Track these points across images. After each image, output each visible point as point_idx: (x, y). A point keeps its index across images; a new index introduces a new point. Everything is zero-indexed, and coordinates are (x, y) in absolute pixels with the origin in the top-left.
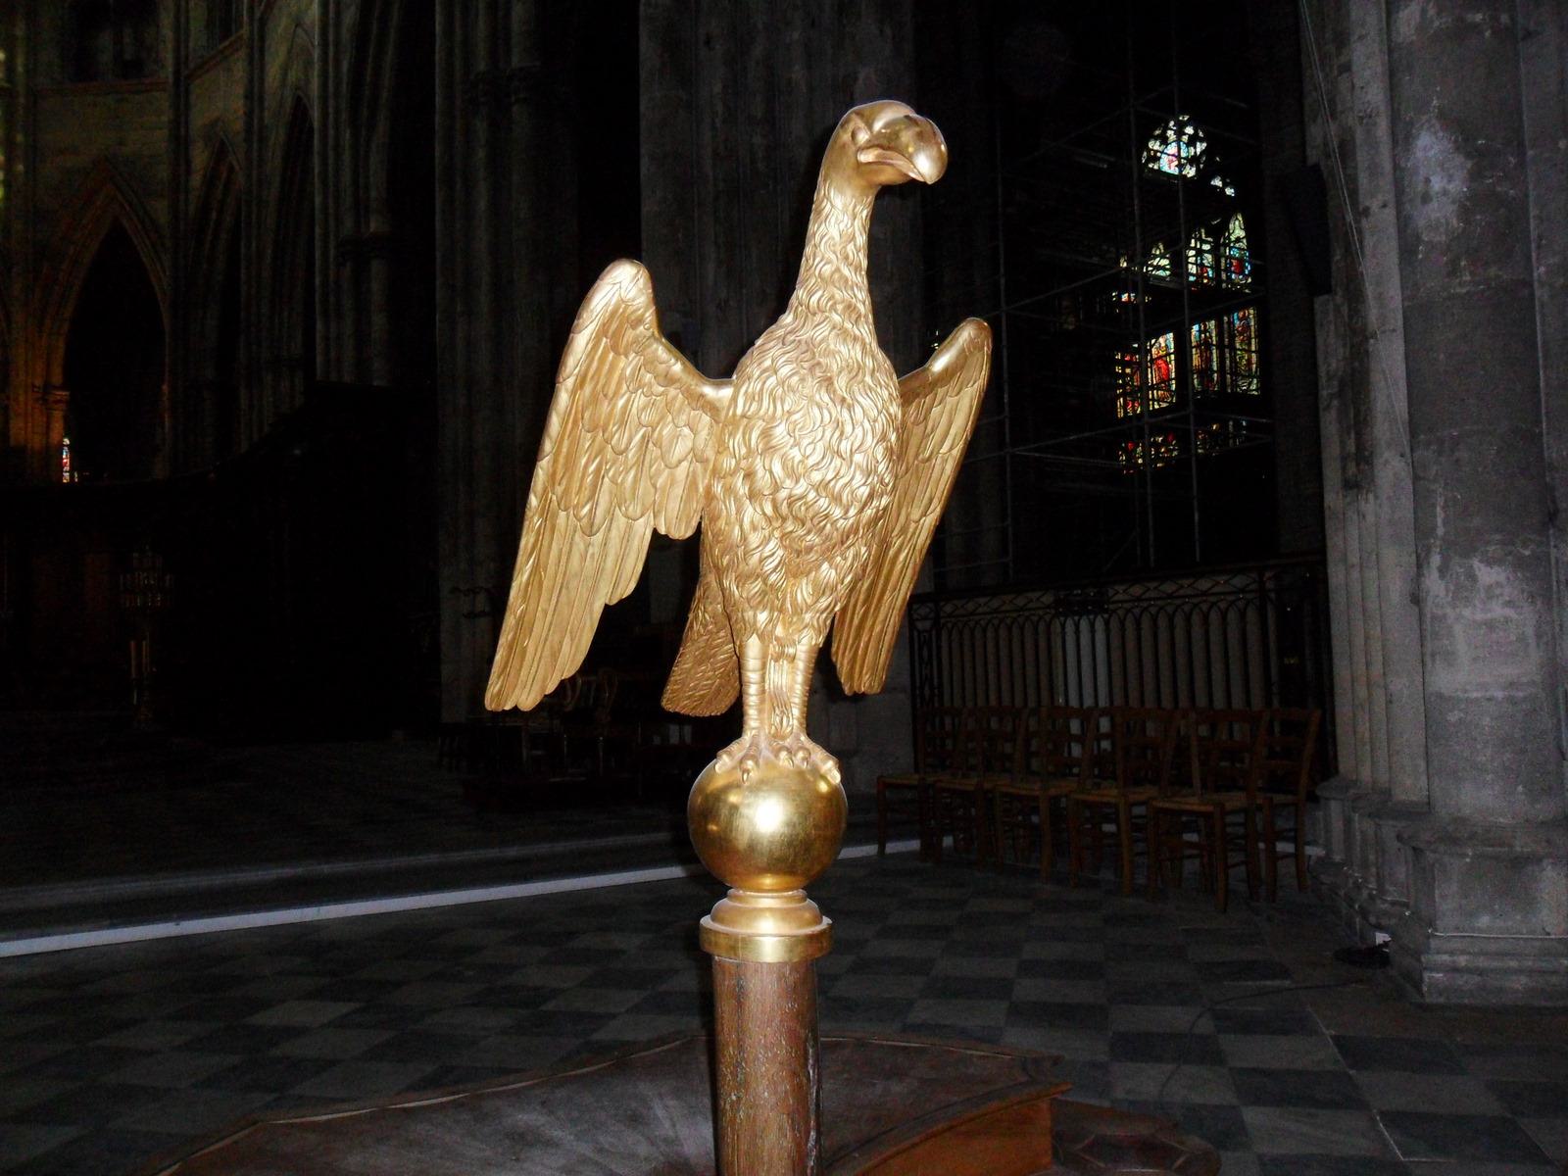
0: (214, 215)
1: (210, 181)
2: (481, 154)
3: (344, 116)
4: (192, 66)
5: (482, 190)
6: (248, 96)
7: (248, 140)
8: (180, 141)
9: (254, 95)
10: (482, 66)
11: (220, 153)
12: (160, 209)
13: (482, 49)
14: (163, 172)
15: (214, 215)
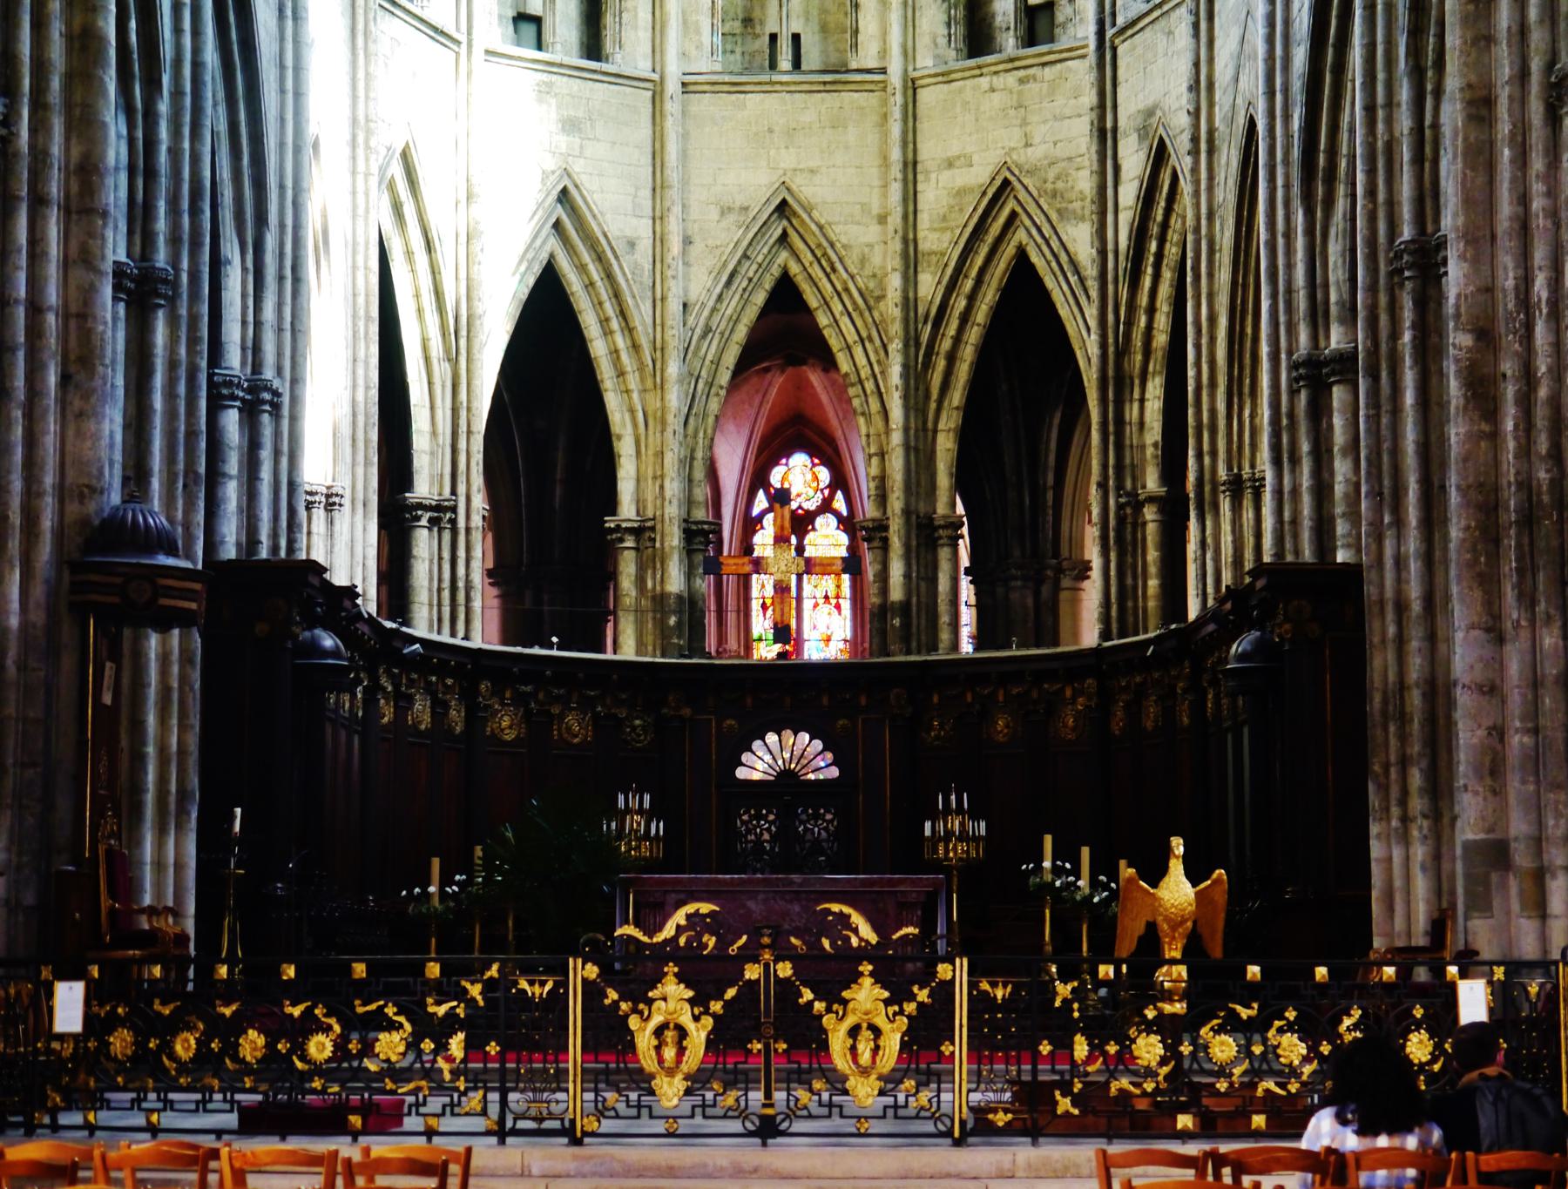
0: (1153, 246)
1: (1147, 199)
2: (1407, 337)
3: (1296, 190)
4: (1120, 21)
5: (1409, 378)
6: (1194, 87)
7: (1194, 152)
8: (1105, 135)
9: (1201, 84)
10: (1407, 233)
11: (1160, 155)
12: (1080, 239)
13: (1406, 212)
14: (1085, 183)
15: (1153, 246)
